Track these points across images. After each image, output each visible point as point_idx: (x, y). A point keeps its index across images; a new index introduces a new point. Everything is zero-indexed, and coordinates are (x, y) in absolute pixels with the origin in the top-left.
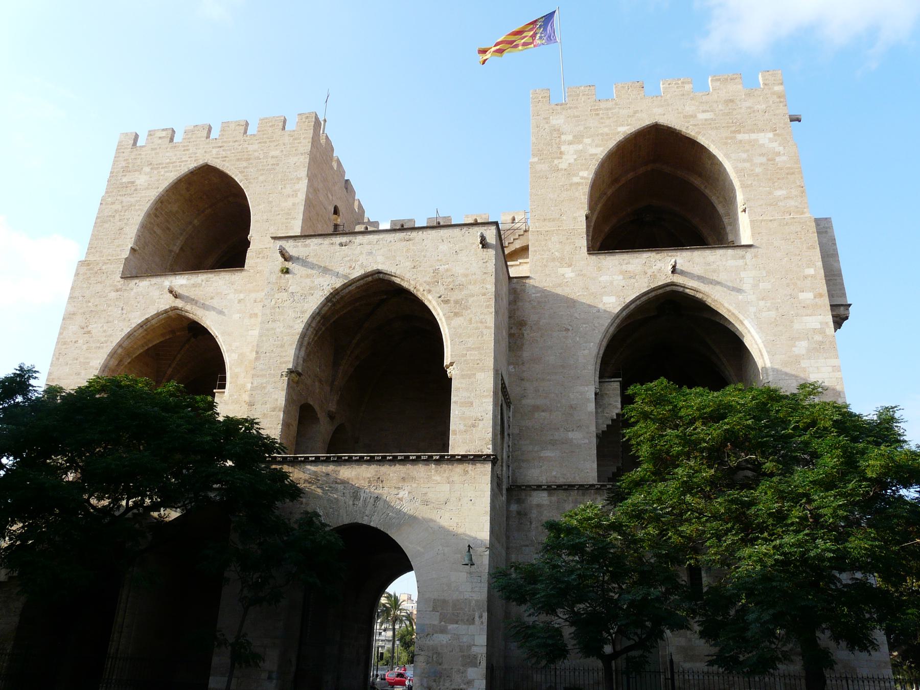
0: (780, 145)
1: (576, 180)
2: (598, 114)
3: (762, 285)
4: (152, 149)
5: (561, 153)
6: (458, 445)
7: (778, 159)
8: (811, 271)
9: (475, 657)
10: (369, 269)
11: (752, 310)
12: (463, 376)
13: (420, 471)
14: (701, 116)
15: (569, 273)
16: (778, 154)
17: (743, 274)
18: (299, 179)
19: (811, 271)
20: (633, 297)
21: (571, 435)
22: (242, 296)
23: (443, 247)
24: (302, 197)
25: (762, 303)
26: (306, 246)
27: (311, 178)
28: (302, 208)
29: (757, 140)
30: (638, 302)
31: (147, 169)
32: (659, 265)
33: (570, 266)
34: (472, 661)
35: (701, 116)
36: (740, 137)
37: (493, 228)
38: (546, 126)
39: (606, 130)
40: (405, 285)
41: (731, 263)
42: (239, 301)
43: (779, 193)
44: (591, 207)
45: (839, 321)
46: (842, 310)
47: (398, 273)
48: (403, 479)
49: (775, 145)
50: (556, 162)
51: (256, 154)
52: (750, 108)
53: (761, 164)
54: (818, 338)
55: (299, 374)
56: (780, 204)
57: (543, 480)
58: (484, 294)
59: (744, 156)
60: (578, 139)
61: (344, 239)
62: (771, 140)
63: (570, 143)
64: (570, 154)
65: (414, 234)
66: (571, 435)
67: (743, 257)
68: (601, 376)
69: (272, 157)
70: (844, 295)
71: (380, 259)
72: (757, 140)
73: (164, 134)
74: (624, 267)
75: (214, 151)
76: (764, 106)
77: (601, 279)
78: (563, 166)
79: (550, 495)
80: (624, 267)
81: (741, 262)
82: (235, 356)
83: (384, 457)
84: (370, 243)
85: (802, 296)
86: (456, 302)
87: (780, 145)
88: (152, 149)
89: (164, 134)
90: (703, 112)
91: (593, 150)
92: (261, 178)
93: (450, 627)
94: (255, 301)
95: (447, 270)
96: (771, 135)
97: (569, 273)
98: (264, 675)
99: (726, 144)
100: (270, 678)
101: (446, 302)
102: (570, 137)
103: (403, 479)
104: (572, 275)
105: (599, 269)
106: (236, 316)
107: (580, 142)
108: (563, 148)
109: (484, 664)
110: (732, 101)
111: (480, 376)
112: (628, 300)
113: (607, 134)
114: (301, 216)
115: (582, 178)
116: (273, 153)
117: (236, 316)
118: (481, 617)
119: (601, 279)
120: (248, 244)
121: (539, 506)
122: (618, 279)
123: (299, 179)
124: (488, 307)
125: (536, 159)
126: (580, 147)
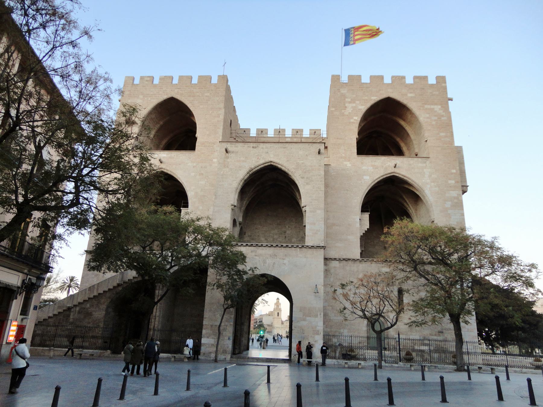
0: (444, 112)
1: (352, 120)
2: (362, 90)
3: (433, 176)
4: (143, 86)
5: (346, 107)
6: (309, 241)
7: (443, 118)
8: (454, 171)
9: (318, 331)
10: (267, 160)
11: (429, 186)
12: (311, 212)
13: (292, 251)
14: (410, 95)
15: (349, 164)
16: (443, 116)
17: (425, 170)
18: (220, 109)
19: (454, 171)
20: (377, 177)
21: (349, 237)
22: (195, 164)
23: (301, 153)
24: (222, 117)
25: (433, 184)
26: (236, 147)
27: (225, 107)
28: (222, 123)
29: (434, 109)
30: (379, 180)
31: (141, 97)
32: (389, 164)
33: (349, 161)
34: (317, 333)
35: (410, 95)
36: (426, 106)
37: (323, 145)
38: (339, 93)
39: (366, 98)
40: (283, 168)
41: (420, 165)
42: (194, 167)
43: (442, 134)
44: (359, 134)
45: (464, 192)
46: (464, 188)
47: (280, 163)
48: (286, 255)
49: (441, 112)
50: (343, 111)
51: (198, 94)
52: (431, 93)
53: (435, 120)
54: (456, 201)
55: (235, 206)
56: (442, 139)
57: (337, 256)
58: (319, 175)
59: (428, 115)
60: (353, 101)
61: (255, 145)
62: (440, 109)
63: (350, 103)
64: (350, 108)
65: (287, 145)
66: (349, 237)
67: (425, 163)
68: (362, 212)
69: (206, 96)
70: (466, 181)
71: (272, 156)
72: (434, 109)
73: (148, 79)
74: (373, 163)
75: (176, 91)
76: (437, 93)
77: (364, 168)
78: (346, 113)
79: (340, 263)
80: (373, 163)
81: (424, 165)
82: (193, 193)
83: (277, 245)
84: (266, 148)
85: (450, 182)
86: (307, 178)
87: (444, 112)
88: (143, 86)
89: (148, 79)
90: (411, 93)
91: (360, 107)
92: (201, 106)
93: (308, 318)
94: (202, 167)
95: (303, 163)
96: (440, 107)
97: (349, 164)
98: (226, 338)
99: (420, 109)
100: (229, 339)
101: (303, 178)
102: (349, 100)
103: (286, 255)
104: (350, 165)
105: (362, 163)
106: (193, 174)
107: (354, 103)
108: (347, 105)
109: (322, 334)
110: (423, 89)
111: (319, 212)
112: (375, 179)
113: (367, 100)
114: (222, 128)
115: (355, 120)
116: (206, 94)
117: (193, 174)
118: (320, 314)
119: (364, 168)
120: (196, 139)
121: (335, 267)
122: (371, 168)
123: (220, 109)
124: (321, 181)
125: (334, 109)
126: (354, 105)
